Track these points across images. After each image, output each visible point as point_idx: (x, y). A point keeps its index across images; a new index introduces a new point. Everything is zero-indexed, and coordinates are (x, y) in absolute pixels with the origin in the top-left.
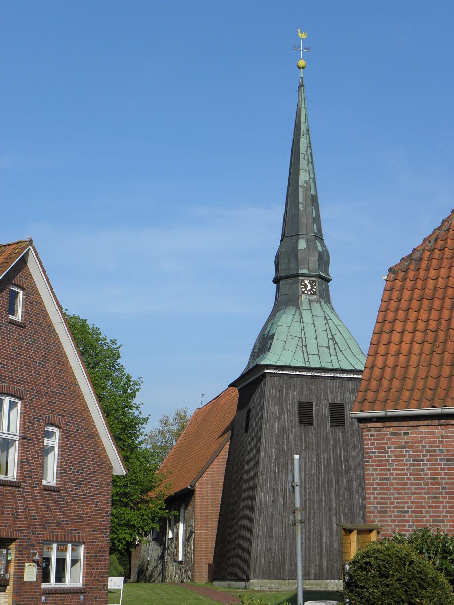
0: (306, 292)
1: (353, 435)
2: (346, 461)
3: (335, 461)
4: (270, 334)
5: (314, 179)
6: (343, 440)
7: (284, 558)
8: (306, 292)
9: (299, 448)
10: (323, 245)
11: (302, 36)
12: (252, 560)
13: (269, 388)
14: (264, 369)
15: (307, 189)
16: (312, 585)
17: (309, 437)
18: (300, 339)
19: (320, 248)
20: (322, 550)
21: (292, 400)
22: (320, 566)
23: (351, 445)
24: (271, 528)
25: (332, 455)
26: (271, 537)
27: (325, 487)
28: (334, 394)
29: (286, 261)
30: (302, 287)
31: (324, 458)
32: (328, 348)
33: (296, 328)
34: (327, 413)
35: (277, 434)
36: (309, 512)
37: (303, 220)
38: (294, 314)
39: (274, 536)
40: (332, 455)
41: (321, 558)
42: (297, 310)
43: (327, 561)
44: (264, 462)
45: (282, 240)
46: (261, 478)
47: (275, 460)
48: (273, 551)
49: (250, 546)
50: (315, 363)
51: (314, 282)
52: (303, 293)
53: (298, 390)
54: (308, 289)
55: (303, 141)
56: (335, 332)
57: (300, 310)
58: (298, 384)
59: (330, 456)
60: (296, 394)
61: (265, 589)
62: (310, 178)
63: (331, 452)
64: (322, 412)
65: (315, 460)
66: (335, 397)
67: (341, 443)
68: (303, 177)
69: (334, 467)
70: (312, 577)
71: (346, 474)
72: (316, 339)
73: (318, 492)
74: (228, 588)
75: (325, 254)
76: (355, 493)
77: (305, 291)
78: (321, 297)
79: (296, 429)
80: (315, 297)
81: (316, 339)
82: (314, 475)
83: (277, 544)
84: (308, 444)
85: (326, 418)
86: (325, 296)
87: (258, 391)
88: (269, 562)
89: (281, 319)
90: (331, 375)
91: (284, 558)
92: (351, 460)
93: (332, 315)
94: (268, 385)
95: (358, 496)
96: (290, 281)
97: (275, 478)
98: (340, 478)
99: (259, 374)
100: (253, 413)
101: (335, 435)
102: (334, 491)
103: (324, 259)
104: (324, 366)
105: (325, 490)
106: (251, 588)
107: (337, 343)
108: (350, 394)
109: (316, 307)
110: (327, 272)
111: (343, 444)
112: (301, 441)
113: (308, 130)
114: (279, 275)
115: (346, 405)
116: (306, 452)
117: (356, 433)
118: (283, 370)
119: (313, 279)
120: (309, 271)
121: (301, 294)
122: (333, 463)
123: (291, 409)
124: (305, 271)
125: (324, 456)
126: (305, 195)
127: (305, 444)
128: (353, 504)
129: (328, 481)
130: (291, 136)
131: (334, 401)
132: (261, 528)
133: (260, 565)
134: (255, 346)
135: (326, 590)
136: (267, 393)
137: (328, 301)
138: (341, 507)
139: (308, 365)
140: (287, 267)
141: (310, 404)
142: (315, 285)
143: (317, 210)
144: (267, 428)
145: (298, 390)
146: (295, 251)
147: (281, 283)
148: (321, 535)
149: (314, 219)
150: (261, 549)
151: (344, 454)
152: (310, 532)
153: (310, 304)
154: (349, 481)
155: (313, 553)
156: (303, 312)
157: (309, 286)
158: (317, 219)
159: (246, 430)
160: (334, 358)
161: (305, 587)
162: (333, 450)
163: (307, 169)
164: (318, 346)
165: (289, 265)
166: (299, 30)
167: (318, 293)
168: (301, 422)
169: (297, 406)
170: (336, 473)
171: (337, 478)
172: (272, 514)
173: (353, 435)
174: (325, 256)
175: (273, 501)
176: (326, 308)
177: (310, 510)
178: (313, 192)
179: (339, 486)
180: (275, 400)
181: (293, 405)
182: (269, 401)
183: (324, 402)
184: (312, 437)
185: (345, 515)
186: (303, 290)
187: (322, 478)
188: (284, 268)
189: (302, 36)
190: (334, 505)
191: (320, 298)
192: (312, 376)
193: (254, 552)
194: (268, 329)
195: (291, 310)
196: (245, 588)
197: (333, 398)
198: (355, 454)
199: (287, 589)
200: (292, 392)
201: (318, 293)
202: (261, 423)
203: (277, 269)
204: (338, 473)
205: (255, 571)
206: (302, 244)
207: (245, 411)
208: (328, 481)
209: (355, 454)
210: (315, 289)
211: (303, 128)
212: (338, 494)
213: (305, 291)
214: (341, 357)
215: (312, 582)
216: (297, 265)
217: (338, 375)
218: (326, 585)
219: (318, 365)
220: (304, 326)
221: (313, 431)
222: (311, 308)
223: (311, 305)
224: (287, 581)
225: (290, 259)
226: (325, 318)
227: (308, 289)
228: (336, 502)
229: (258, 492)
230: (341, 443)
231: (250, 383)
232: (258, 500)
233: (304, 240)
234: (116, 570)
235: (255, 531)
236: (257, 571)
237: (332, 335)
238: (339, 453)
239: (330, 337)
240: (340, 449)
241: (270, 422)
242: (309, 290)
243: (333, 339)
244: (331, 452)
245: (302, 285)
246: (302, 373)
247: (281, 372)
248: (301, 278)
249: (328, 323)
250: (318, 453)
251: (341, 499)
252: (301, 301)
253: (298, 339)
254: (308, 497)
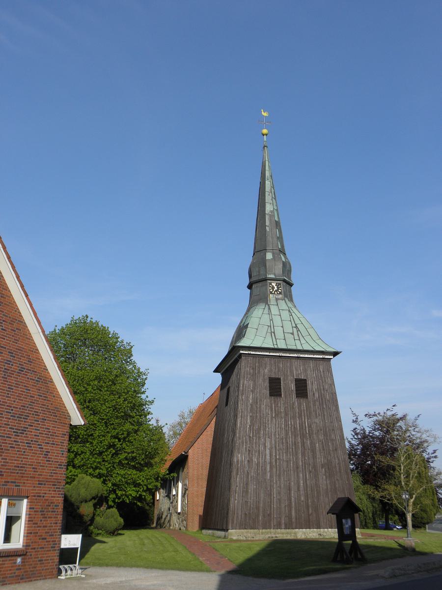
0: (273, 292)
2: (310, 426)
5: (277, 210)
6: (307, 409)
7: (258, 510)
8: (273, 292)
9: (270, 415)
10: (286, 258)
11: (265, 114)
12: (230, 513)
13: (244, 367)
14: (239, 351)
15: (272, 216)
16: (283, 534)
17: (278, 407)
18: (269, 328)
19: (283, 259)
20: (291, 502)
21: (264, 376)
22: (289, 517)
23: (313, 414)
24: (247, 484)
25: (298, 422)
26: (247, 492)
27: (292, 449)
28: (298, 371)
29: (257, 269)
32: (293, 334)
33: (266, 319)
34: (293, 387)
35: (251, 405)
36: (280, 470)
37: (269, 239)
39: (250, 491)
40: (298, 422)
41: (290, 511)
43: (296, 512)
44: (240, 428)
45: (254, 254)
46: (238, 442)
47: (250, 426)
48: (249, 505)
49: (229, 500)
53: (268, 368)
54: (275, 290)
56: (297, 321)
58: (268, 363)
59: (296, 423)
60: (267, 371)
61: (242, 538)
64: (289, 386)
67: (305, 412)
68: (269, 208)
69: (300, 432)
70: (283, 526)
71: (310, 437)
72: (282, 327)
73: (287, 453)
74: (212, 536)
75: (288, 264)
76: (318, 453)
78: (286, 296)
79: (267, 401)
80: (280, 296)
81: (282, 327)
82: (283, 439)
83: (252, 498)
86: (289, 296)
87: (236, 370)
88: (246, 514)
90: (295, 355)
91: (258, 510)
92: (314, 426)
94: (243, 364)
96: (260, 284)
97: (250, 442)
98: (305, 440)
99: (236, 356)
100: (231, 390)
101: (300, 405)
102: (300, 452)
103: (287, 268)
104: (290, 347)
105: (292, 451)
106: (229, 537)
108: (311, 371)
109: (283, 305)
110: (290, 278)
111: (307, 412)
112: (272, 410)
117: (317, 403)
119: (279, 282)
121: (269, 293)
123: (263, 383)
124: (272, 276)
126: (270, 220)
127: (275, 412)
129: (295, 444)
130: (259, 180)
132: (238, 484)
133: (237, 517)
135: (295, 538)
136: (242, 371)
137: (291, 300)
138: (306, 465)
139: (276, 347)
140: (258, 273)
141: (279, 379)
142: (280, 287)
145: (268, 368)
146: (263, 262)
147: (253, 286)
148: (290, 490)
149: (278, 238)
150: (238, 502)
151: (308, 421)
152: (280, 487)
153: (277, 301)
154: (313, 444)
155: (283, 506)
156: (271, 307)
157: (276, 287)
158: (280, 238)
159: (227, 405)
160: (297, 342)
161: (277, 535)
165: (259, 272)
166: (262, 110)
167: (283, 293)
168: (271, 395)
172: (248, 472)
174: (288, 266)
175: (248, 461)
176: (290, 305)
177: (280, 468)
178: (276, 219)
180: (249, 376)
181: (264, 381)
182: (244, 377)
184: (280, 407)
185: (310, 472)
186: (271, 290)
187: (290, 441)
188: (255, 274)
189: (265, 114)
190: (301, 464)
191: (285, 297)
192: (279, 356)
193: (232, 505)
194: (243, 322)
196: (225, 537)
198: (317, 421)
199: (261, 538)
203: (250, 277)
204: (303, 436)
205: (233, 523)
206: (269, 256)
207: (226, 390)
208: (295, 444)
209: (317, 421)
211: (267, 174)
212: (303, 454)
214: (303, 341)
215: (283, 531)
217: (301, 356)
218: (295, 533)
219: (284, 347)
221: (281, 402)
224: (261, 531)
226: (289, 311)
227: (275, 290)
228: (302, 461)
229: (236, 453)
231: (228, 367)
232: (235, 460)
234: (117, 521)
235: (233, 487)
236: (235, 522)
237: (296, 325)
238: (303, 420)
240: (305, 417)
243: (296, 327)
245: (270, 287)
246: (271, 354)
247: (254, 353)
248: (269, 281)
249: (291, 315)
251: (306, 458)
254: (278, 457)
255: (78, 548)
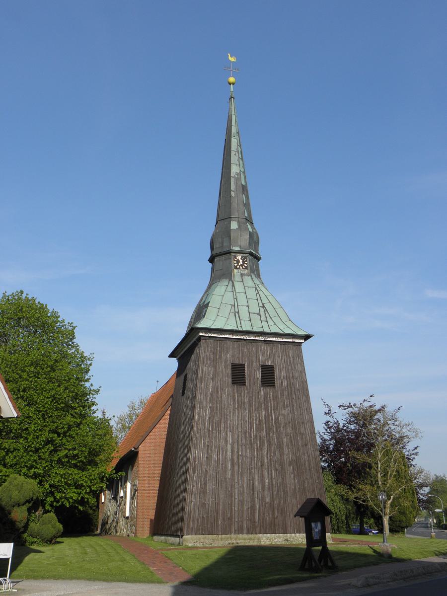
0: (238, 267)
1: (282, 394)
2: (277, 418)
3: (267, 419)
4: (205, 304)
5: (244, 173)
6: (273, 399)
7: (217, 513)
8: (238, 267)
9: (232, 406)
10: (253, 227)
11: (232, 59)
12: (186, 516)
13: (203, 351)
14: (199, 333)
15: (238, 179)
16: (245, 539)
17: (241, 397)
18: (233, 307)
19: (250, 229)
20: (254, 504)
21: (226, 362)
22: (252, 521)
23: (281, 404)
24: (205, 484)
25: (263, 413)
26: (205, 492)
27: (257, 444)
28: (265, 356)
29: (220, 240)
30: (234, 262)
31: (256, 416)
32: (259, 314)
33: (229, 296)
34: (258, 374)
35: (211, 394)
36: (242, 468)
37: (234, 205)
38: (227, 286)
39: (208, 491)
40: (263, 413)
41: (253, 513)
42: (230, 282)
43: (260, 515)
44: (198, 420)
45: (217, 223)
46: (195, 436)
47: (209, 418)
48: (207, 506)
49: (184, 502)
50: (246, 327)
51: (245, 258)
52: (236, 267)
53: (231, 352)
54: (239, 264)
55: (234, 142)
56: (265, 300)
57: (233, 282)
58: (231, 347)
59: (262, 415)
60: (230, 356)
61: (198, 545)
62: (240, 171)
63: (263, 410)
64: (254, 373)
65: (247, 418)
66: (265, 360)
67: (272, 402)
68: (235, 170)
69: (266, 425)
70: (245, 531)
71: (277, 431)
72: (248, 306)
73: (250, 449)
74: (165, 543)
75: (255, 235)
76: (285, 449)
77: (237, 266)
78: (252, 271)
79: (228, 390)
80: (246, 271)
81: (248, 306)
82: (246, 432)
83: (211, 500)
84: (240, 403)
85: (258, 378)
86: (255, 271)
87: (194, 356)
88: (203, 517)
89: (216, 290)
90: (262, 339)
91: (217, 513)
92: (281, 418)
93: (261, 286)
94: (202, 348)
95: (289, 451)
96: (223, 257)
97: (209, 436)
98: (271, 435)
99: (195, 339)
100: (189, 377)
101: (266, 395)
102: (265, 447)
103: (254, 239)
104: (255, 329)
105: (257, 446)
106: (184, 544)
107: (267, 310)
108: (279, 357)
109: (248, 281)
110: (257, 251)
111: (274, 403)
112: (234, 400)
113: (238, 133)
114: (214, 253)
115: (276, 367)
116: (238, 410)
117: (286, 393)
118: (217, 334)
119: (245, 255)
120: (241, 248)
121: (233, 267)
122: (264, 420)
123: (224, 370)
124: (237, 248)
125: (256, 414)
126: (236, 184)
127: (238, 403)
128: (284, 460)
129: (260, 438)
130: (224, 137)
131: (265, 363)
132: (195, 484)
133: (194, 521)
134: (191, 318)
135: (258, 544)
136: (202, 356)
137: (258, 276)
138: (272, 463)
139: (240, 329)
140: (221, 245)
141: (243, 365)
142: (246, 261)
143: (247, 198)
144: (201, 388)
145: (231, 352)
146: (227, 232)
147: (216, 260)
148: (253, 490)
149: (245, 204)
150: (194, 505)
151: (274, 413)
152: (242, 487)
153: (242, 277)
154: (279, 438)
155: (245, 508)
156: (236, 284)
157: (241, 261)
158: (247, 205)
159: (183, 394)
160: (264, 324)
161: (238, 541)
162: (265, 409)
163: (238, 163)
164: (249, 313)
165: (222, 243)
166: (229, 54)
167: (249, 268)
168: (234, 383)
169: (230, 367)
170: (268, 430)
171: (268, 435)
172: (206, 470)
173: (282, 394)
174: (255, 237)
175: (207, 457)
176: (257, 281)
177: (242, 466)
178: (243, 183)
179: (270, 442)
180: (209, 362)
181: (226, 367)
182: (204, 363)
183: (255, 364)
184: (244, 397)
185: (276, 470)
186: (236, 265)
187: (254, 435)
188: (218, 246)
189: (232, 59)
190: (266, 461)
191: (251, 273)
192: (244, 339)
193: (187, 508)
194: (203, 300)
195: (225, 282)
196: (179, 544)
197: (264, 361)
198: (285, 412)
199: (220, 545)
200: (226, 355)
201: (249, 268)
202: (196, 385)
203: (212, 249)
204: (269, 430)
205: (188, 527)
206: (234, 225)
207: (182, 377)
208: (260, 438)
209: (285, 412)
210: (246, 264)
211: (234, 130)
212: (269, 450)
213: (237, 266)
214: (271, 323)
215: (245, 536)
216: (230, 243)
217: (269, 339)
218: (259, 539)
219: (249, 329)
220: (237, 295)
221: (245, 391)
222: (242, 280)
223: (243, 278)
224: (220, 536)
225: (224, 238)
226: (256, 289)
227: (239, 264)
228: (268, 458)
229: (193, 449)
230: (272, 402)
231: (185, 351)
232: (192, 457)
233: (236, 222)
234: (54, 528)
235: (189, 487)
236: (191, 526)
237: (263, 304)
238: (270, 411)
239: (261, 305)
240: (271, 408)
241: (205, 383)
242: (241, 265)
243: (263, 307)
244: (263, 410)
245: (235, 261)
246: (234, 337)
247: (215, 335)
248: (234, 254)
249: (258, 293)
250: (250, 411)
251: (272, 454)
252: (234, 275)
253: (231, 306)
254: (240, 453)
255: (9, 559)
